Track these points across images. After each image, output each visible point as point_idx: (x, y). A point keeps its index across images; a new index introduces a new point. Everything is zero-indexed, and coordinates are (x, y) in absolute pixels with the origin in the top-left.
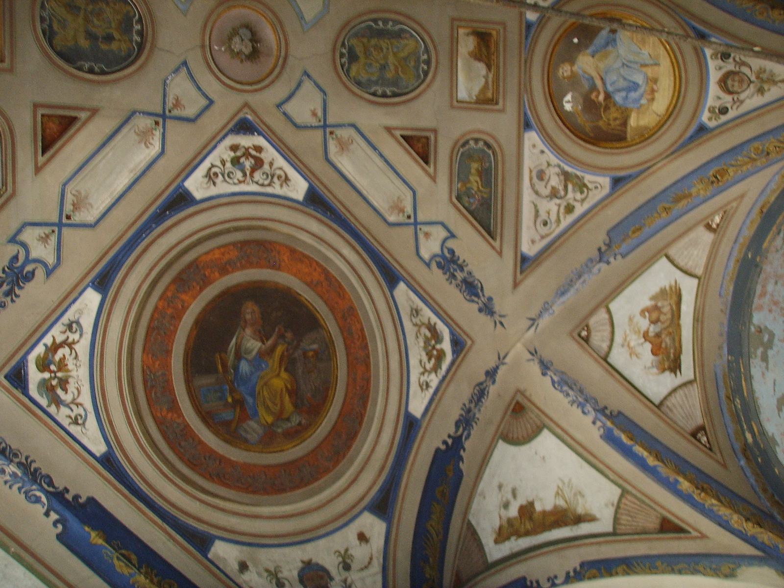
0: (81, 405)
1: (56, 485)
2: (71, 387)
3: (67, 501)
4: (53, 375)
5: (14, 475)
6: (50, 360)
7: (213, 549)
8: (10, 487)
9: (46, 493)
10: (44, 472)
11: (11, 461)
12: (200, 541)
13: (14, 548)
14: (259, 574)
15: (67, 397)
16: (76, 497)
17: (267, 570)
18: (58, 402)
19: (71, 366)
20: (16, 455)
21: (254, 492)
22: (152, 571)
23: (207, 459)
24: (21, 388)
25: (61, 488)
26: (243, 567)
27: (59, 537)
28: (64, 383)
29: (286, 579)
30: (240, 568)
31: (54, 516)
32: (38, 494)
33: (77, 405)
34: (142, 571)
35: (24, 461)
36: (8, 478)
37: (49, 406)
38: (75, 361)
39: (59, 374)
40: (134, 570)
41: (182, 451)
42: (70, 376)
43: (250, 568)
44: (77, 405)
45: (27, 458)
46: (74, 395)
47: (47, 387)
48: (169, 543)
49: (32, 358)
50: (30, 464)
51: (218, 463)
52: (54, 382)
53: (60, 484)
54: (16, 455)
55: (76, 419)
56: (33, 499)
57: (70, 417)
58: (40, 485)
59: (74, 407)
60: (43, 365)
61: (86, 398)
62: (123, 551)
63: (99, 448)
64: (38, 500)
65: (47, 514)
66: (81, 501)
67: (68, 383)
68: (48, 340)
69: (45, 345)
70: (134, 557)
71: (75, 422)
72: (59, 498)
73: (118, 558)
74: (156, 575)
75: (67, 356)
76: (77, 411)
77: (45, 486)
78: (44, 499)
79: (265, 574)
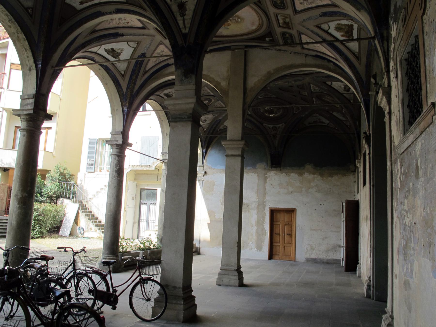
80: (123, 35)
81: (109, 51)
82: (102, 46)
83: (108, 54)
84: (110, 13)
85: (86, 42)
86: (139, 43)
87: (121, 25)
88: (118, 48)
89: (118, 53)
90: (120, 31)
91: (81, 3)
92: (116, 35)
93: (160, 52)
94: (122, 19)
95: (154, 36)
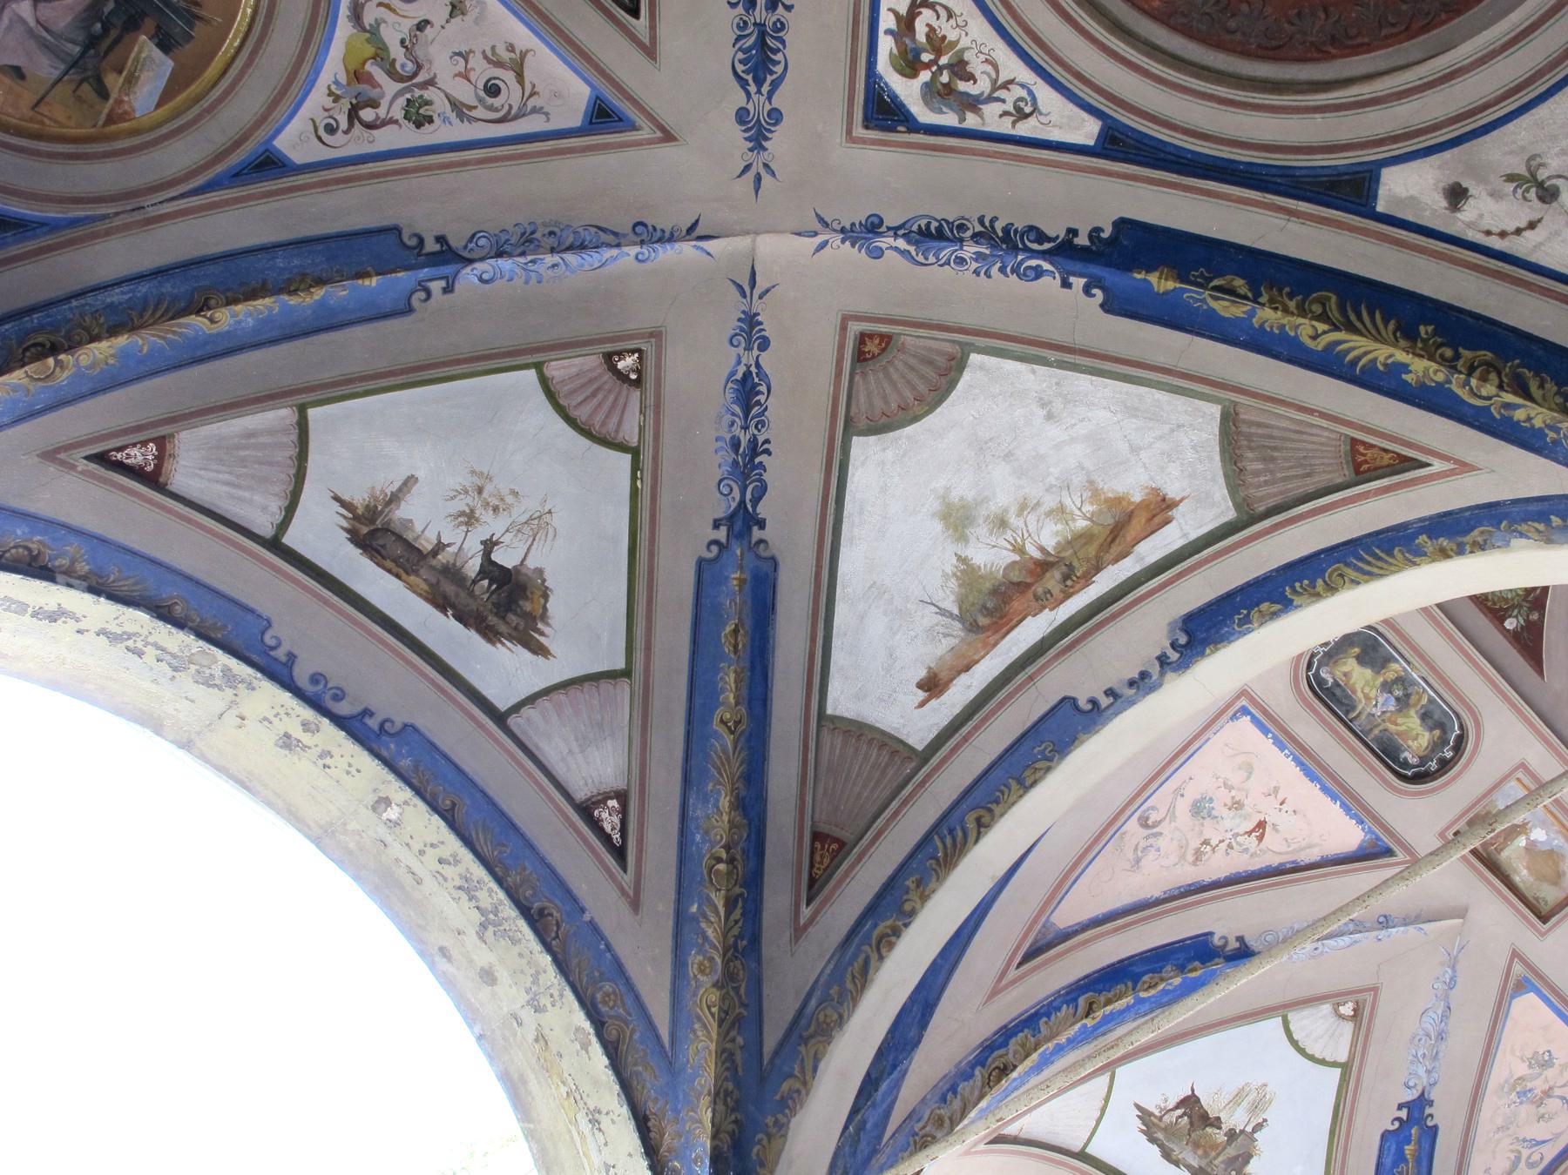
0: (1011, 82)
1: (1051, 233)
2: (976, 66)
3: (1084, 249)
4: (934, 68)
5: (979, 257)
6: (913, 50)
7: (1382, 192)
8: (989, 277)
9: (1043, 255)
10: (1020, 225)
11: (961, 240)
12: (1348, 190)
13: (1052, 355)
14: (1495, 195)
15: (982, 86)
16: (1095, 233)
17: (1511, 178)
18: (972, 104)
19: (952, 35)
20: (962, 227)
21: (1426, 29)
22: (1280, 291)
23: (1297, 21)
24: (901, 122)
25: (1062, 235)
26: (1456, 195)
27: (1106, 307)
28: (960, 69)
29: (1559, 176)
30: (1450, 203)
31: (1078, 283)
32: (1033, 263)
33: (1006, 85)
34: (1261, 300)
35: (979, 228)
36: (975, 265)
37: (963, 119)
38: (952, 22)
39: (944, 60)
40: (1249, 306)
41: (1238, 37)
42: (963, 50)
43: (1472, 191)
44: (1006, 85)
45: (981, 221)
46: (989, 75)
47: (938, 94)
48: (1290, 225)
49: (883, 65)
50: (992, 227)
51: (1323, 16)
52: (945, 78)
53: (1056, 229)
54: (962, 227)
55: (1019, 110)
56: (1032, 274)
57: (1006, 113)
58: (1026, 249)
59: (1000, 94)
60: (909, 64)
61: (1012, 67)
62: (1216, 282)
63: (1086, 131)
64: (1039, 273)
65: (1066, 284)
66: (1105, 235)
67: (967, 63)
68: (887, 21)
69: (888, 32)
70: (1239, 283)
71: (1021, 115)
72: (1066, 252)
73: (1216, 299)
74: (1291, 296)
75: (935, 24)
76: (1010, 96)
77: (1035, 246)
78: (1046, 266)
79: (1511, 187)
80: (1243, 953)
81: (1170, 1130)
82: (1121, 1071)
83: (1167, 1155)
84: (1142, 683)
85: (1006, 1034)
86: (1360, 1009)
87: (1218, 866)
88: (1231, 1090)
89: (1232, 1135)
90: (1221, 919)
91: (933, 685)
92: (1202, 956)
93: (1521, 1069)
94: (1220, 810)
95: (1461, 913)
